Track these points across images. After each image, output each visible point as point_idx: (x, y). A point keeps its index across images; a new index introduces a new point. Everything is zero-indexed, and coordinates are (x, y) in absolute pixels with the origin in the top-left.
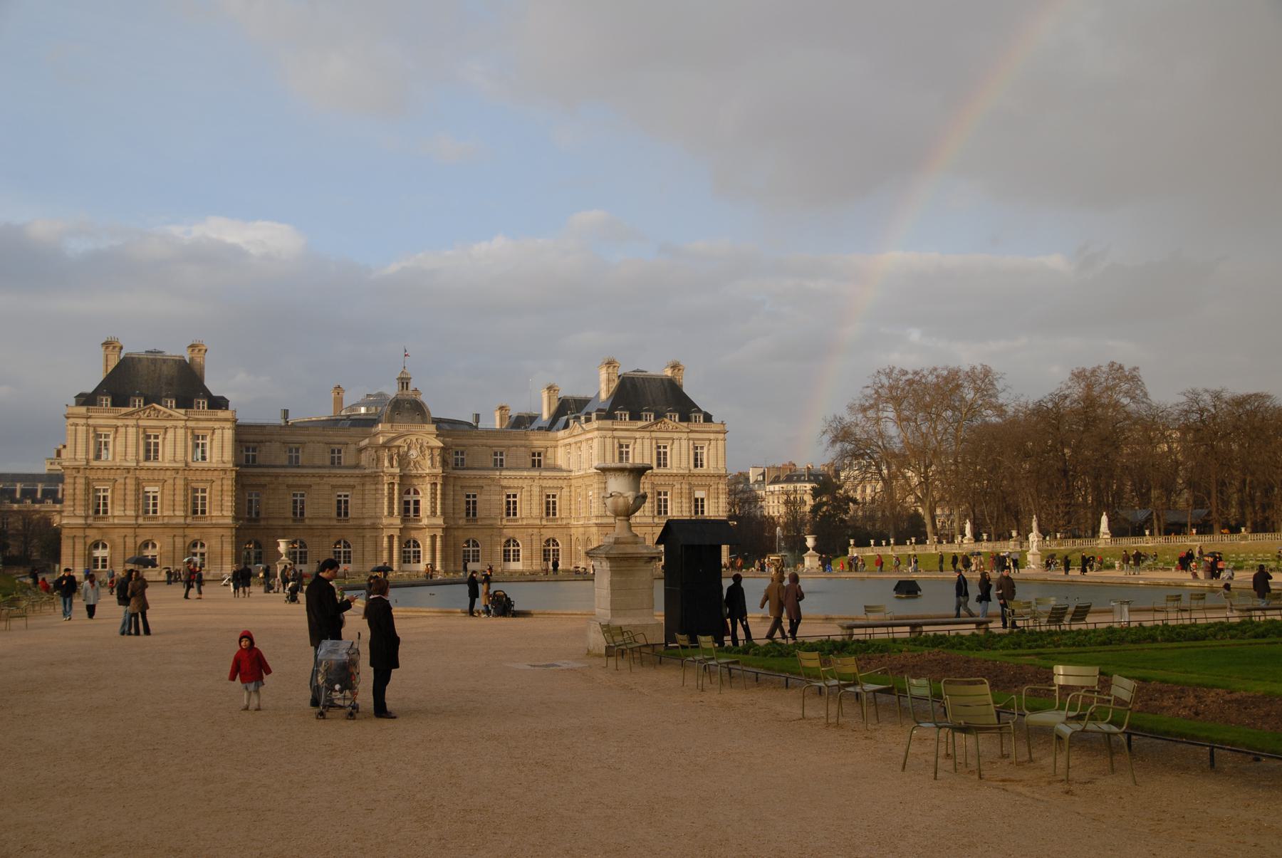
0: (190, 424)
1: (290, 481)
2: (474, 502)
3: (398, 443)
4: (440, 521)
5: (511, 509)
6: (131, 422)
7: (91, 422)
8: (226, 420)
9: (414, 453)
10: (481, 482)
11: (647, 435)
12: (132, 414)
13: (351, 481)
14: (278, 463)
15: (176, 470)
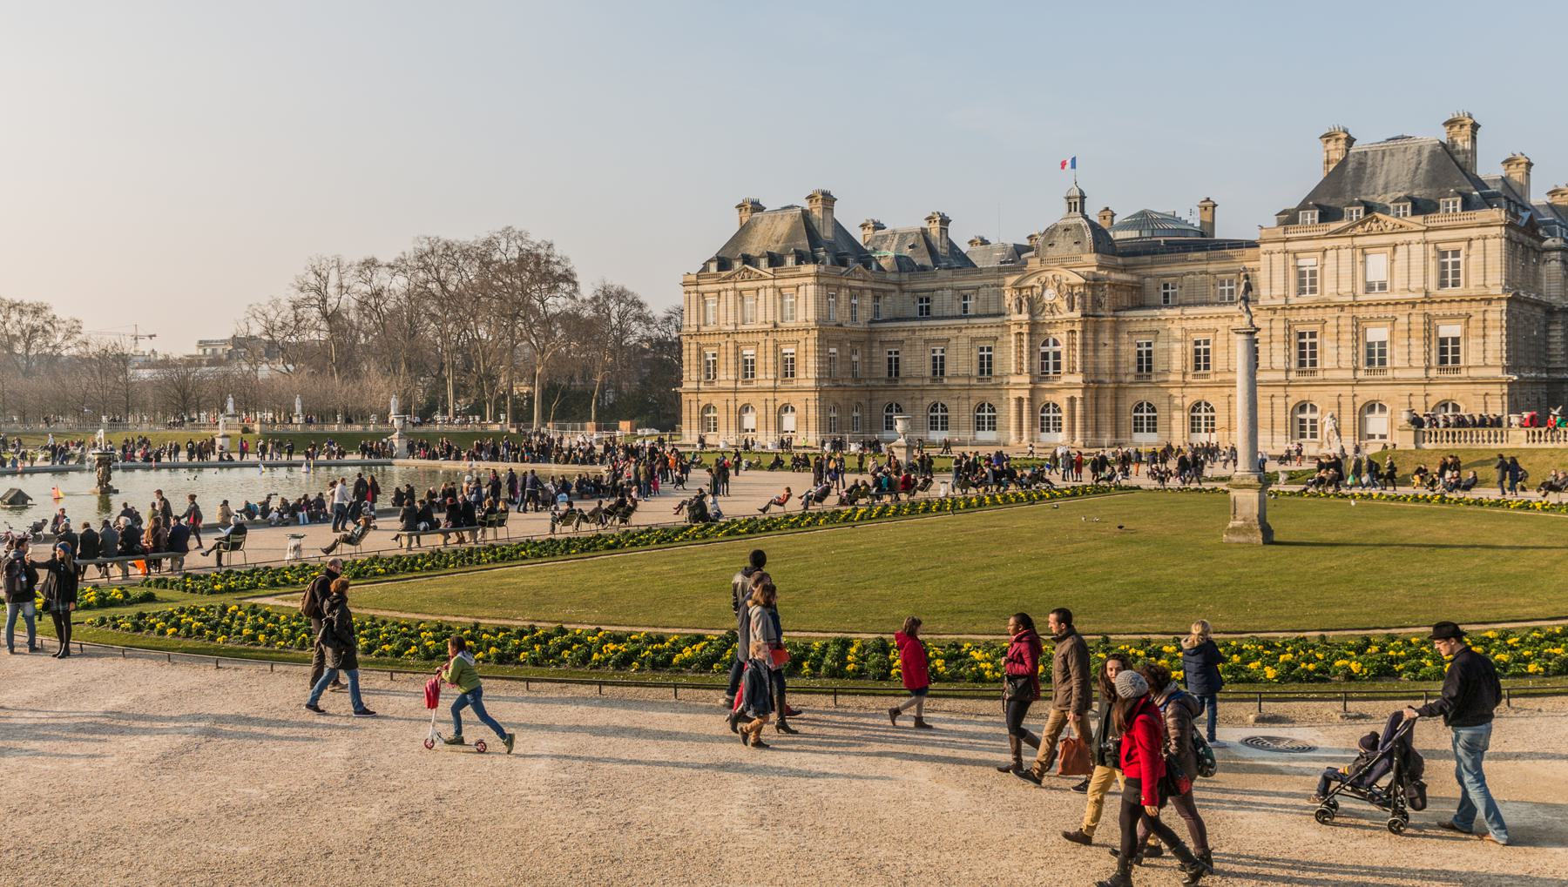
0: (779, 283)
1: (927, 335)
2: (1149, 353)
3: (1031, 282)
4: (1078, 378)
5: (1201, 360)
6: (730, 286)
7: (701, 288)
8: (808, 275)
9: (1050, 295)
10: (1155, 326)
11: (1347, 242)
12: (729, 277)
13: (992, 332)
14: (949, 313)
15: (767, 332)
